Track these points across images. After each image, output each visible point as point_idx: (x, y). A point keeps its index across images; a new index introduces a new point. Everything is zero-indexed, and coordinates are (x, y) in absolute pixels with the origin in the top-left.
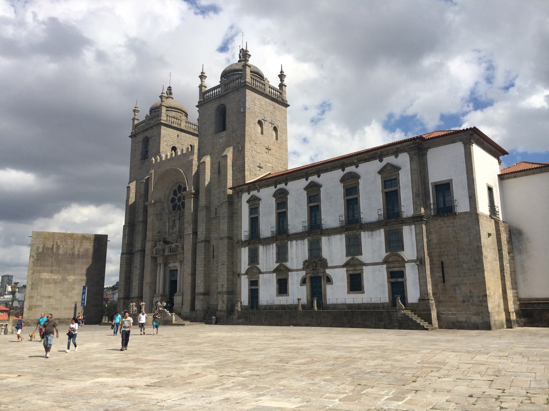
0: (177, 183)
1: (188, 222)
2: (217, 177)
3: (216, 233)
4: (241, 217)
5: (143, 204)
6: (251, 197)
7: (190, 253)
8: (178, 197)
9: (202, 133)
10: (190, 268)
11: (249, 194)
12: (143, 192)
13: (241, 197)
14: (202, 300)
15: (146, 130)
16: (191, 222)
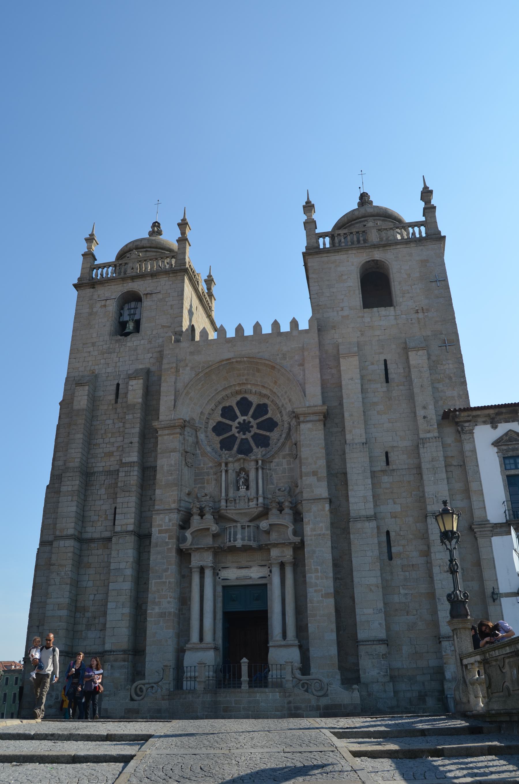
0: (238, 393)
1: (315, 473)
2: (385, 389)
3: (395, 503)
4: (477, 472)
5: (138, 425)
6: (506, 434)
7: (329, 543)
8: (239, 423)
9: (321, 303)
10: (332, 579)
11: (495, 427)
12: (140, 400)
13: (471, 432)
14: (385, 654)
15: (133, 278)
16: (323, 473)
